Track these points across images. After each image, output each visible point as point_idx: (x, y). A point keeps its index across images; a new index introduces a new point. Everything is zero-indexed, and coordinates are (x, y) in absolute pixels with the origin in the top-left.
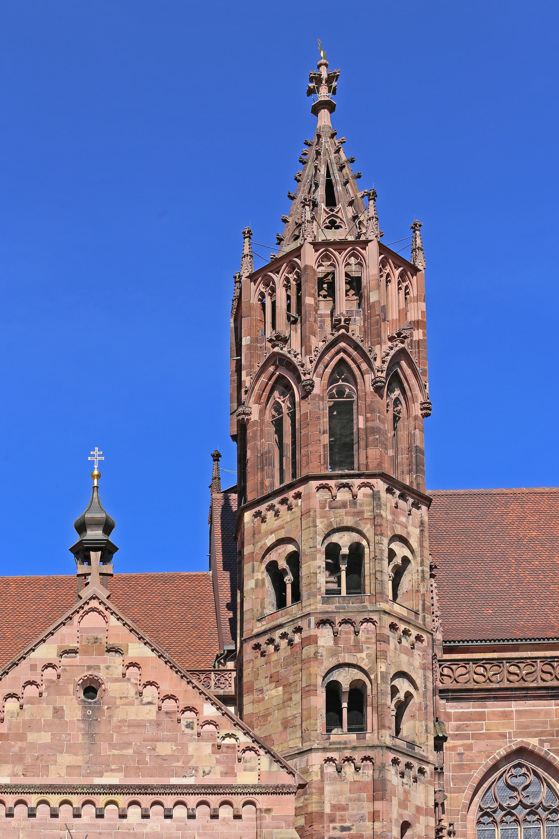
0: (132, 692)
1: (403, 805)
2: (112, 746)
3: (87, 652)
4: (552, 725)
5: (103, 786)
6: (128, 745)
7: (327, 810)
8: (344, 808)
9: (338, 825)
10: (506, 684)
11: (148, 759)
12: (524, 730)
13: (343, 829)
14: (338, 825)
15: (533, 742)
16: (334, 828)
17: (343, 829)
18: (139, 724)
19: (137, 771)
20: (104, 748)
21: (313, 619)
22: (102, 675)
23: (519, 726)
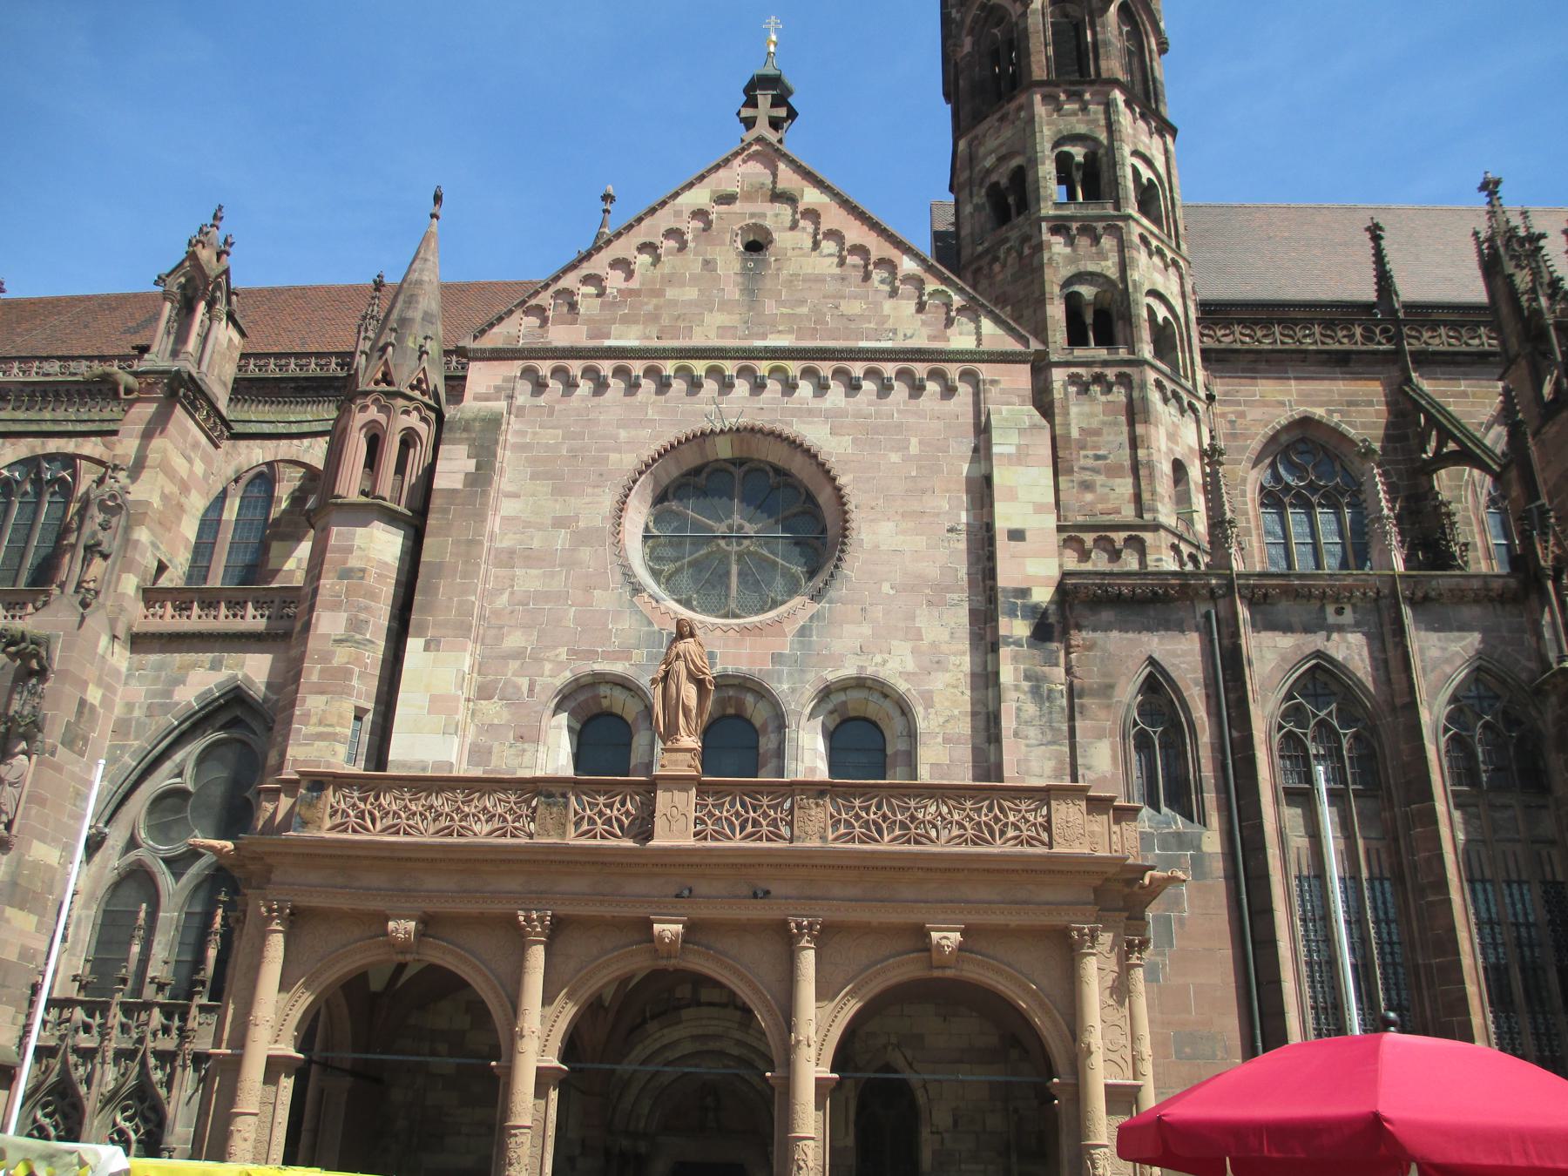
0: (809, 243)
1: (1172, 437)
2: (780, 303)
3: (749, 197)
4: (1340, 394)
5: (766, 349)
6: (803, 302)
7: (1075, 433)
8: (1097, 433)
9: (1090, 453)
10: (1279, 346)
11: (828, 318)
12: (1305, 398)
13: (1097, 457)
14: (1090, 453)
15: (1319, 412)
16: (1086, 457)
17: (1097, 457)
18: (819, 279)
19: (813, 333)
20: (770, 307)
21: (1044, 225)
22: (768, 223)
23: (1300, 393)
